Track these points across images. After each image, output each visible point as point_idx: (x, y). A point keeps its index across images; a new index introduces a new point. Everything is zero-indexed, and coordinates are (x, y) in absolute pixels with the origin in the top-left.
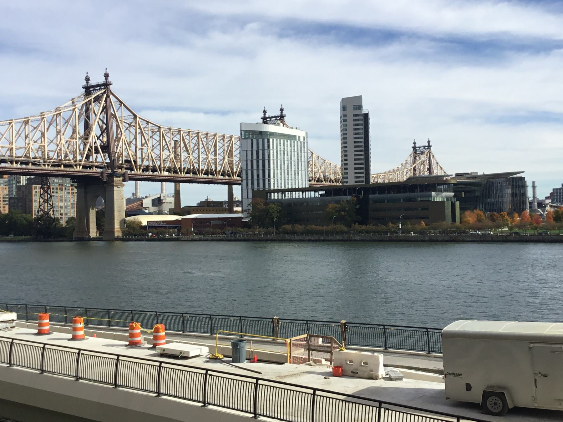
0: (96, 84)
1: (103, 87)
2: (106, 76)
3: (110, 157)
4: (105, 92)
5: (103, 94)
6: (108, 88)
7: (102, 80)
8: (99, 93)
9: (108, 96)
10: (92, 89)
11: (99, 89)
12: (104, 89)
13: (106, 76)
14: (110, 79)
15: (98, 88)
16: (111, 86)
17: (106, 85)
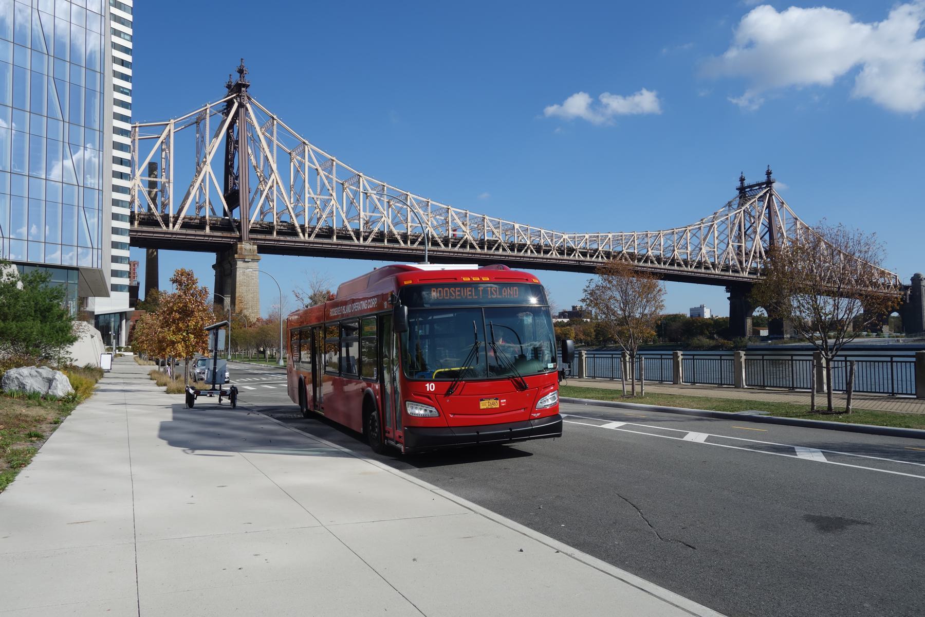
0: (755, 183)
1: (765, 186)
2: (769, 173)
3: (774, 263)
4: (767, 192)
5: (765, 194)
6: (771, 187)
7: (764, 178)
8: (761, 194)
9: (771, 195)
10: (747, 190)
11: (759, 189)
12: (765, 188)
13: (769, 173)
14: (772, 177)
15: (757, 187)
16: (774, 185)
17: (769, 183)
